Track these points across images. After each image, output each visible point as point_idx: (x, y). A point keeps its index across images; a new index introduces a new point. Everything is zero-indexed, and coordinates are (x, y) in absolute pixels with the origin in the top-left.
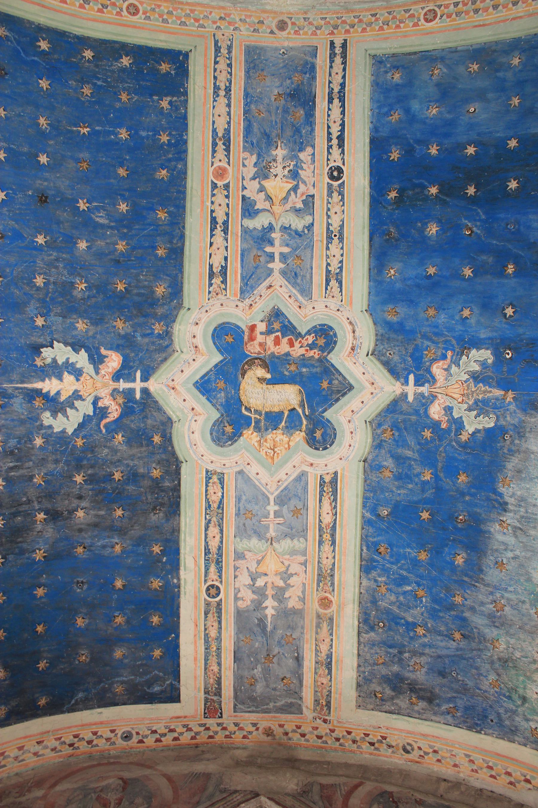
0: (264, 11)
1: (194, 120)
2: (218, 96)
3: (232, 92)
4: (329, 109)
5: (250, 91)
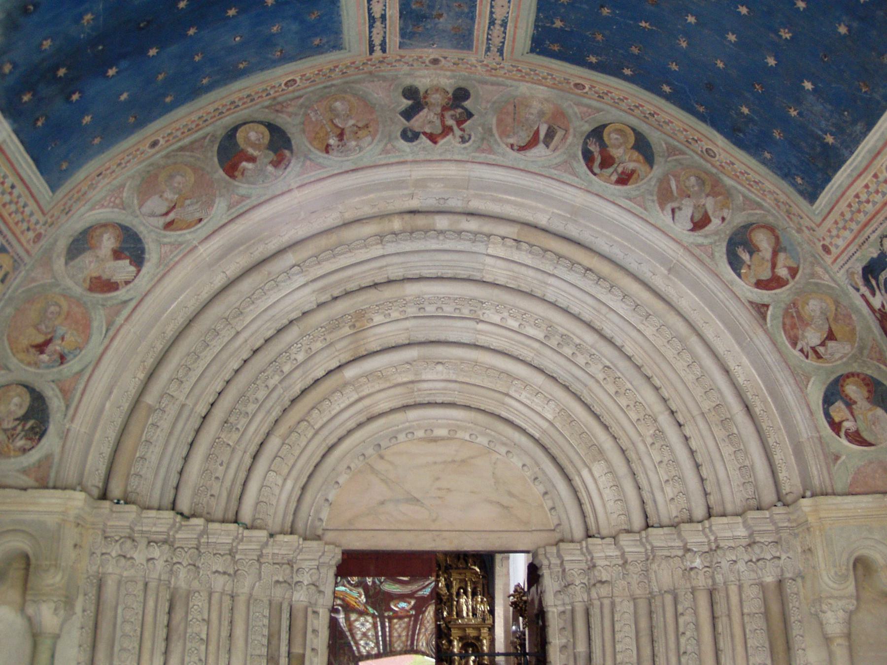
0: (452, 71)
1: (530, 6)
2: (503, 20)
3: (487, 21)
4: (385, 10)
5: (469, 21)
